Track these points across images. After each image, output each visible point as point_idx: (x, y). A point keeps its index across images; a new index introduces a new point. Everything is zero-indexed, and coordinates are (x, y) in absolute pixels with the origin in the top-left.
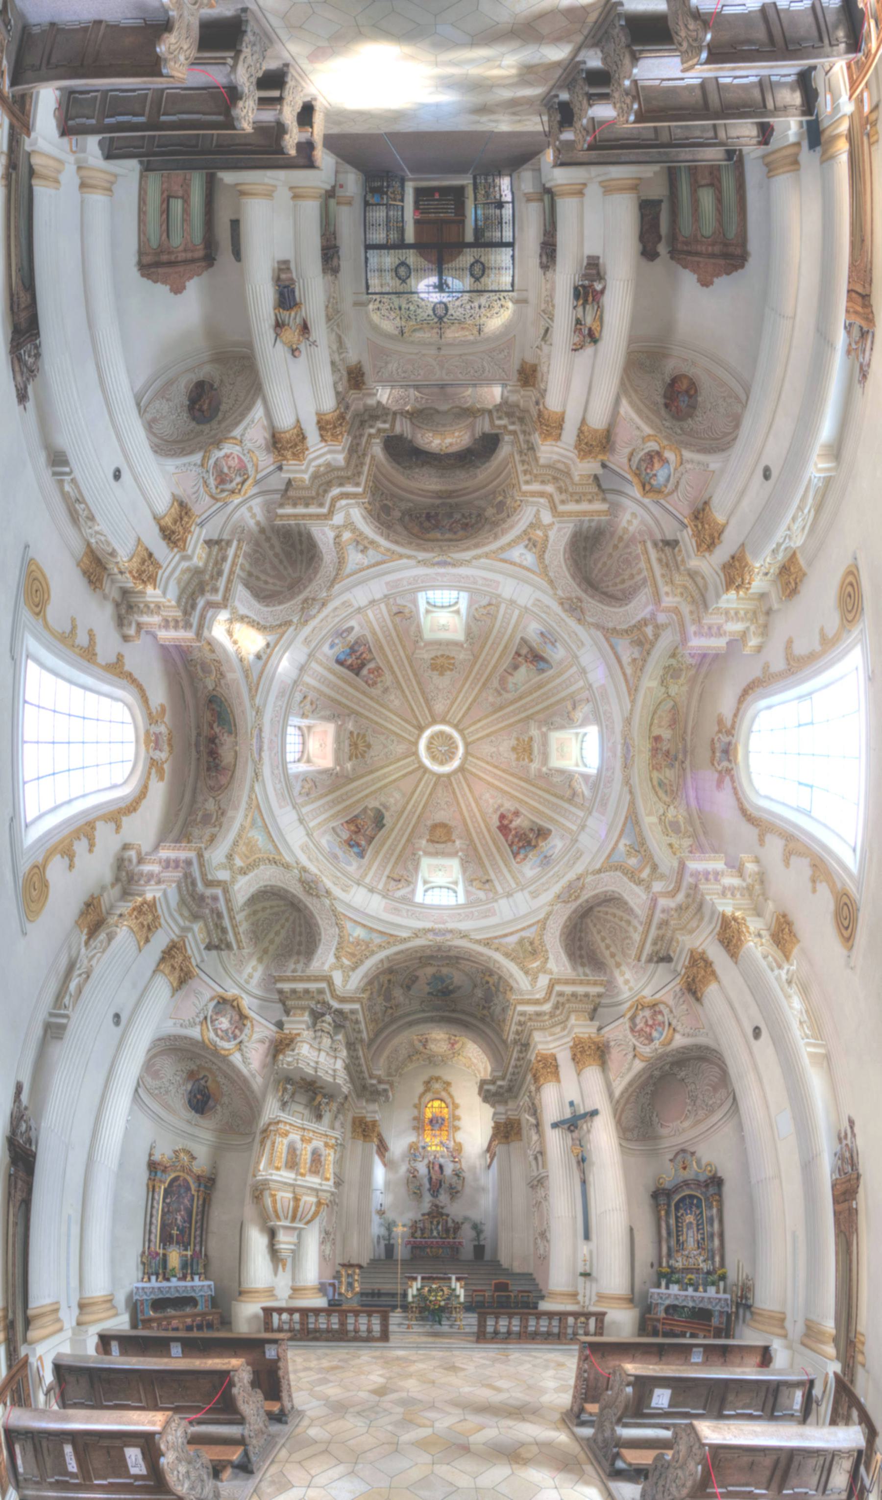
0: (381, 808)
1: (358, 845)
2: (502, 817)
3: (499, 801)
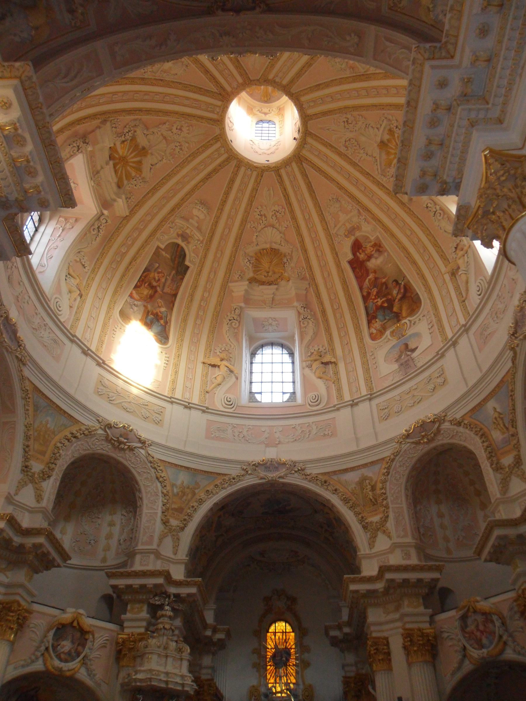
0: (179, 241)
2: (357, 246)
3: (355, 220)
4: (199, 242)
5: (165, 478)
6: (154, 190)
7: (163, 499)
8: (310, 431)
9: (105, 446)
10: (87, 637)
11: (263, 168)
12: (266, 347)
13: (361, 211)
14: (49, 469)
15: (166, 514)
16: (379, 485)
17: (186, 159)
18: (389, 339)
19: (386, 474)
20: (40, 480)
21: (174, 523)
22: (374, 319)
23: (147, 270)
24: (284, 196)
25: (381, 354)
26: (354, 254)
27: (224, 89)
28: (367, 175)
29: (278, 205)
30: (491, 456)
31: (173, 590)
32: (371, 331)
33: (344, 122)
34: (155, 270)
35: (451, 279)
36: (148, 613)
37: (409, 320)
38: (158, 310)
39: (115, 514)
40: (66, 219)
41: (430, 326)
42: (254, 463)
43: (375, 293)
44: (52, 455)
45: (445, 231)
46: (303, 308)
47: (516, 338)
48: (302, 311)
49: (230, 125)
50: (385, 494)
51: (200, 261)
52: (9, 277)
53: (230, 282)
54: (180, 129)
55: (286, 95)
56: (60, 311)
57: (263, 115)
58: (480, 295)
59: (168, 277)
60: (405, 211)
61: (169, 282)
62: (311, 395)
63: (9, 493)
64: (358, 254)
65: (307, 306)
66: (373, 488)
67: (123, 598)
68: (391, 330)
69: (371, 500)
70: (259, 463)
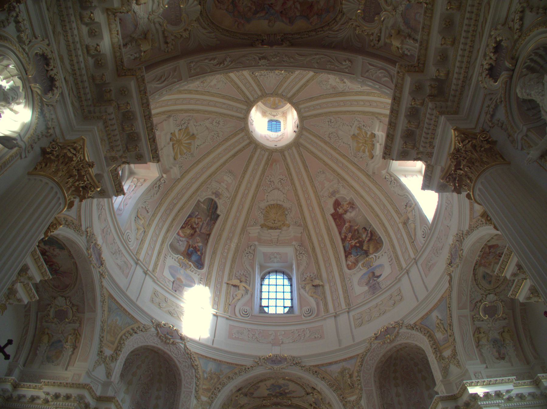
0: (213, 197)
1: (196, 250)
2: (337, 204)
4: (227, 199)
6: (199, 161)
8: (304, 335)
9: (155, 340)
11: (273, 150)
12: (272, 274)
13: (339, 179)
14: (117, 355)
16: (356, 374)
17: (221, 142)
18: (361, 269)
19: (360, 366)
20: (110, 362)
22: (349, 254)
23: (190, 216)
24: (287, 169)
25: (355, 280)
26: (335, 209)
27: (249, 99)
28: (343, 156)
29: (283, 176)
30: (436, 351)
32: (348, 263)
33: (328, 122)
34: (196, 217)
35: (404, 227)
37: (375, 256)
38: (196, 245)
40: (138, 180)
41: (390, 260)
42: (264, 357)
43: (350, 237)
45: (399, 195)
46: (299, 246)
47: (452, 266)
48: (298, 248)
49: (251, 121)
50: (359, 380)
51: (228, 211)
52: (99, 216)
53: (248, 227)
54: (219, 123)
55: (290, 104)
56: (130, 242)
57: (273, 117)
58: (424, 238)
59: (204, 222)
60: (370, 181)
61: (206, 224)
62: (305, 309)
63: (89, 370)
64: (338, 209)
65: (301, 245)
66: (351, 376)
68: (363, 262)
69: (349, 384)
70: (267, 358)
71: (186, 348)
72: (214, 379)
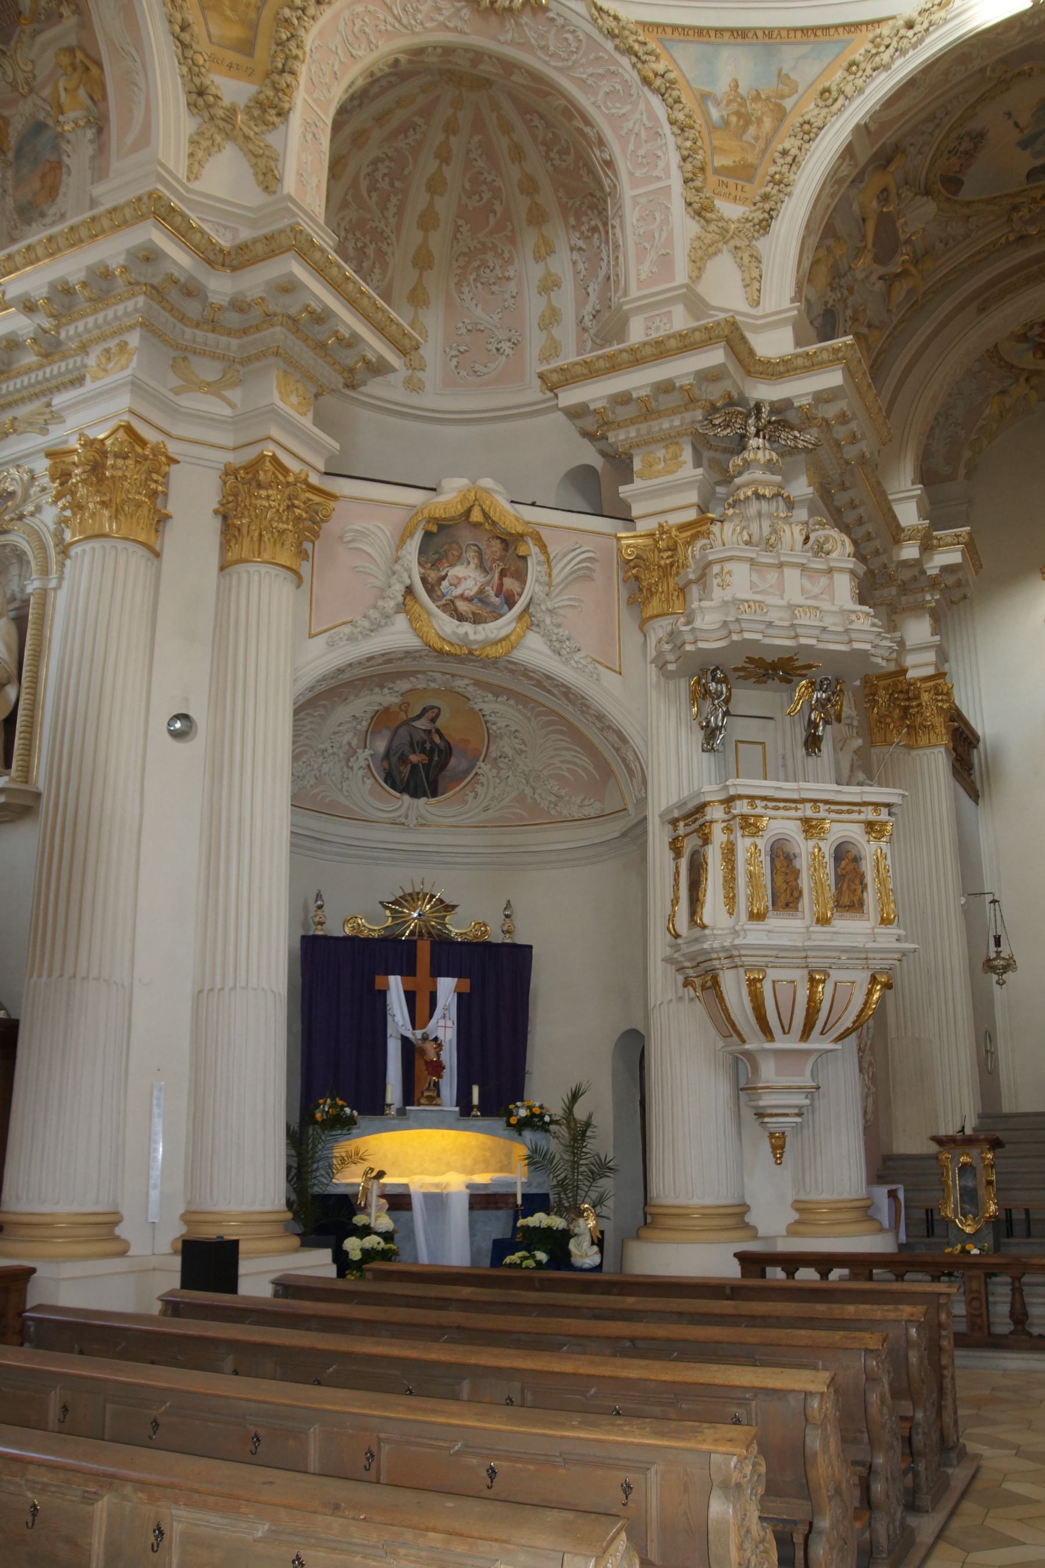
5: (671, 76)
7: (679, 140)
9: (446, 13)
10: (522, 551)
14: (277, 90)
15: (698, 183)
21: (730, 210)
31: (766, 392)
36: (698, 464)
39: (551, 251)
44: (274, 47)
67: (611, 440)
71: (594, 11)
72: (759, 121)
